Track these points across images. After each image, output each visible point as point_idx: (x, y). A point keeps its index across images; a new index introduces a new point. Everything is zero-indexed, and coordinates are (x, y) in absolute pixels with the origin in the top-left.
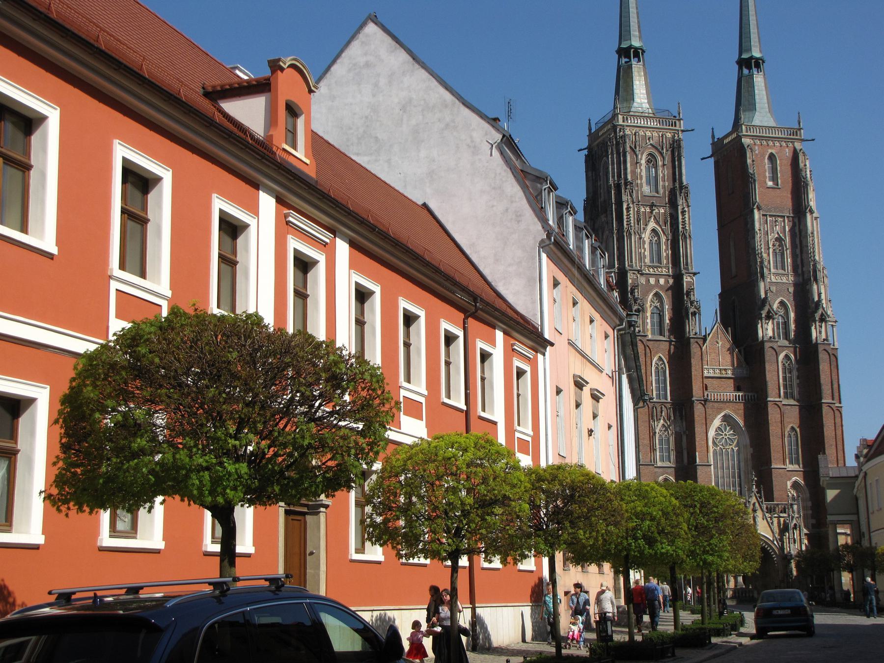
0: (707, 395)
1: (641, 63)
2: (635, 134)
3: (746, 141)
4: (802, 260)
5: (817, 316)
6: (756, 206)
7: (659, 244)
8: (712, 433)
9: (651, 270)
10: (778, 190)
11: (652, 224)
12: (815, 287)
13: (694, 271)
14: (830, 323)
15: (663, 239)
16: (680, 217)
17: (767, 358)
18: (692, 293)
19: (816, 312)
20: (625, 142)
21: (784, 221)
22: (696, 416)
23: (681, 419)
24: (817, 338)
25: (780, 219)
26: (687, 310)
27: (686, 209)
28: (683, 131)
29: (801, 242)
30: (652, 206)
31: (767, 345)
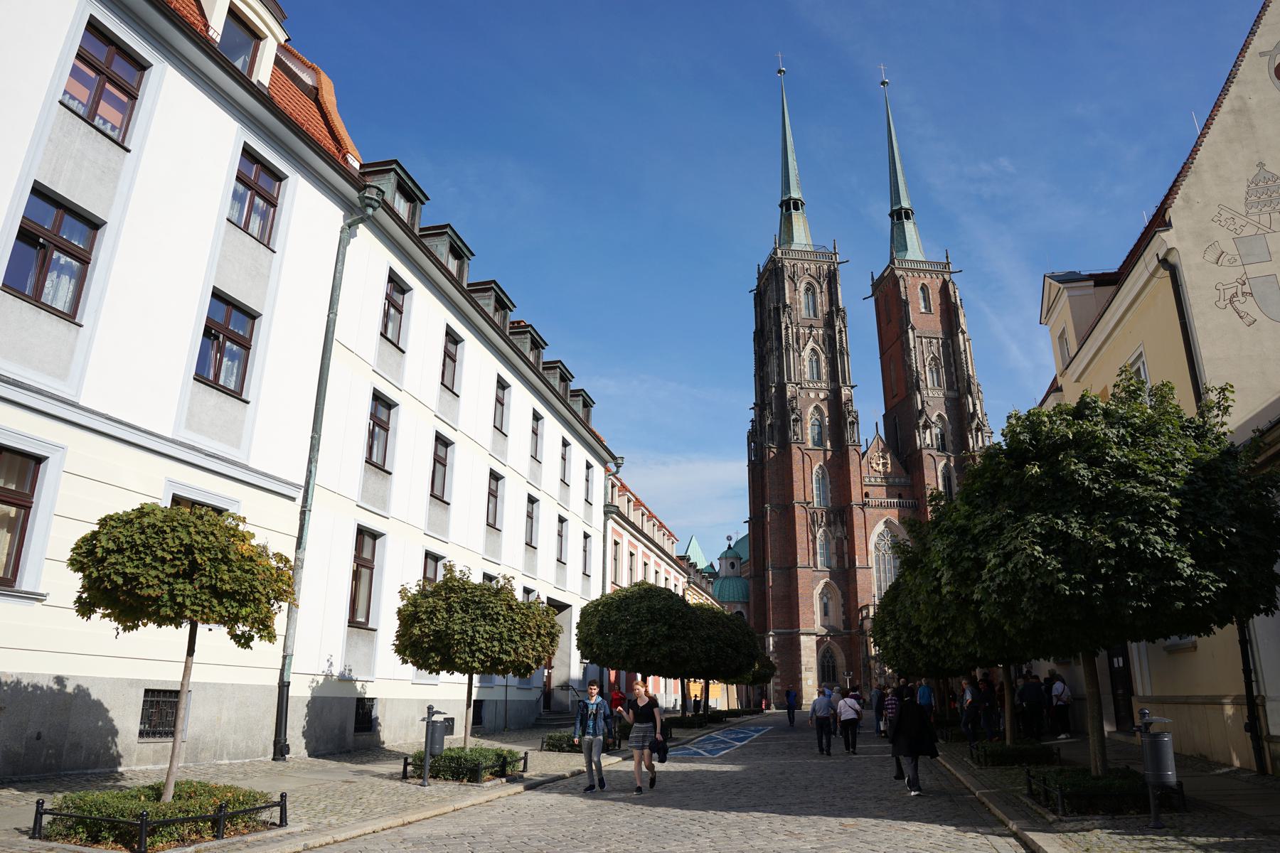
0: (868, 501)
1: (801, 211)
2: (793, 266)
3: (898, 273)
4: (957, 377)
5: (974, 425)
6: (909, 327)
7: (818, 361)
8: (873, 539)
9: (811, 385)
10: (931, 315)
11: (811, 344)
12: (970, 399)
13: (852, 384)
14: (986, 434)
15: (823, 357)
16: (837, 337)
17: (925, 464)
18: (850, 404)
19: (972, 422)
20: (783, 271)
21: (938, 343)
22: (855, 520)
23: (842, 525)
24: (973, 447)
25: (935, 341)
26: (846, 419)
27: (843, 329)
28: (838, 263)
29: (955, 360)
30: (811, 327)
31: (925, 452)
